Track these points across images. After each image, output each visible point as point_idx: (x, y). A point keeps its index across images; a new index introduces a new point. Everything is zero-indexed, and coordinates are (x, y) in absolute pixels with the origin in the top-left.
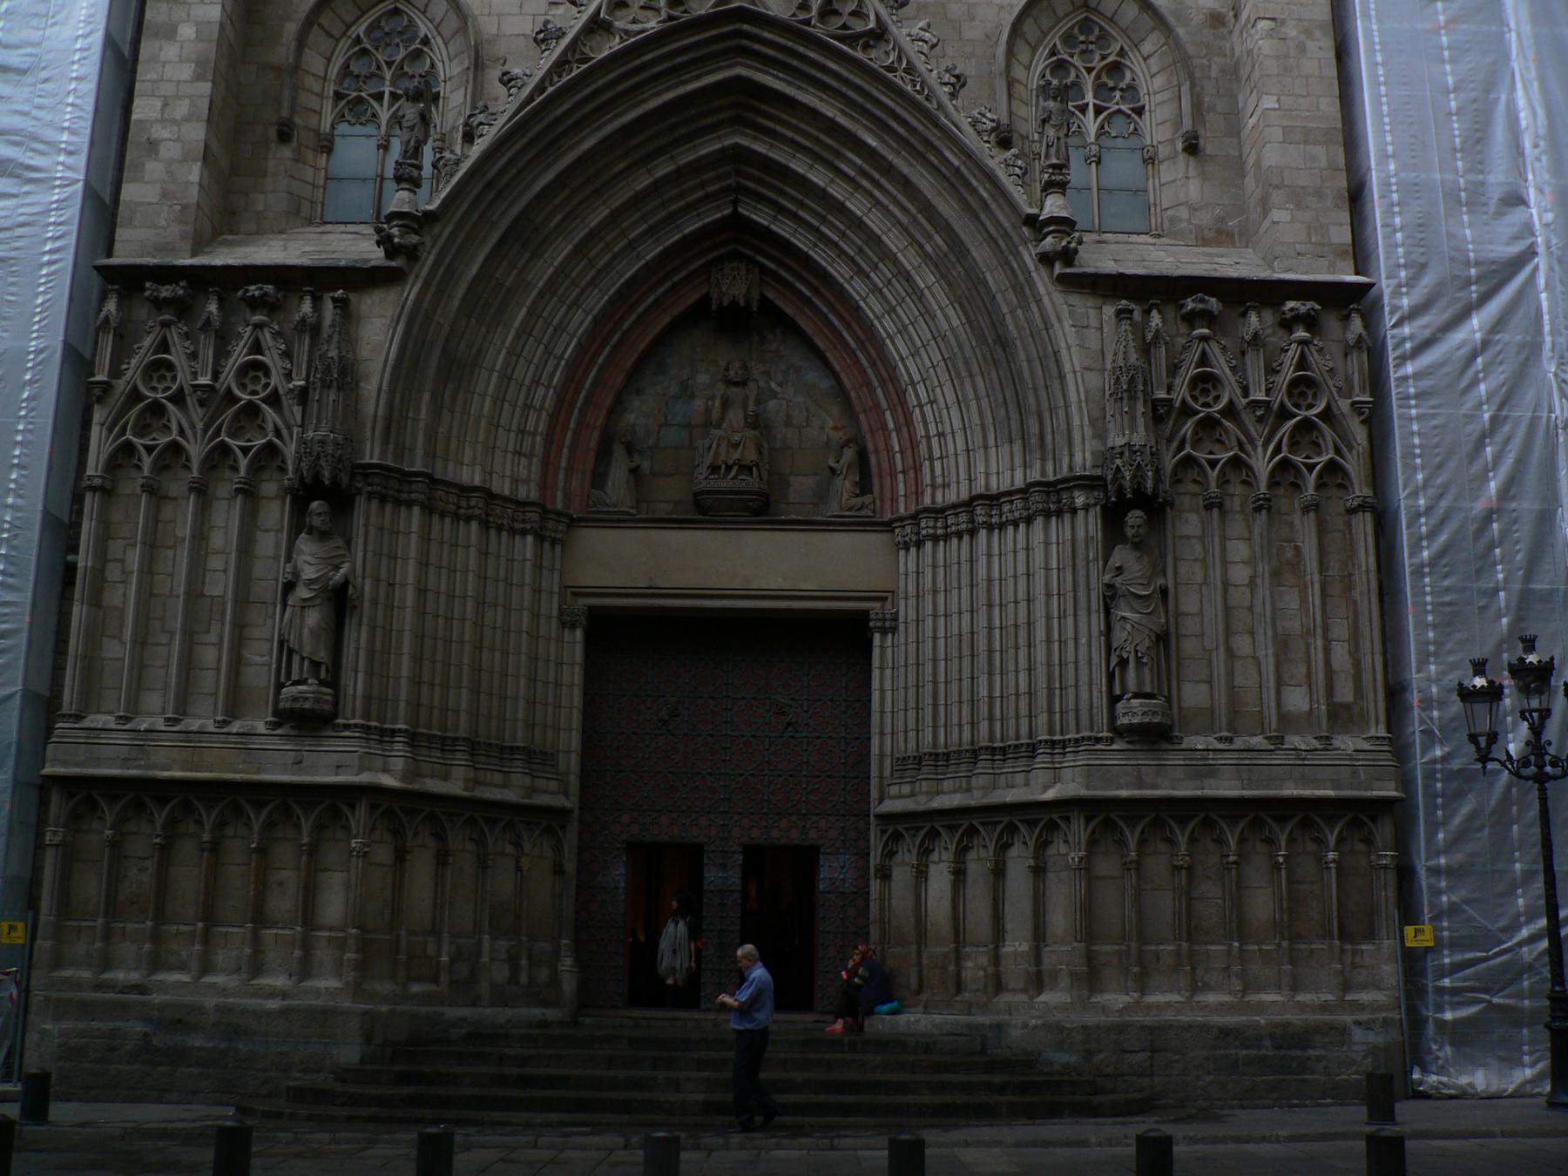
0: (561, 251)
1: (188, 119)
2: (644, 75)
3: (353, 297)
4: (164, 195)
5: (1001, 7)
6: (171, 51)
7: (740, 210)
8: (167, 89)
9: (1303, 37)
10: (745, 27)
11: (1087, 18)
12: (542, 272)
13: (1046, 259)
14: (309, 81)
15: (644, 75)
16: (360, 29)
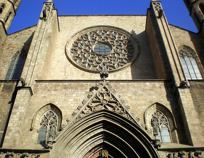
0: (76, 147)
1: (17, 126)
2: (89, 120)
3: (41, 155)
4: (11, 138)
5: (144, 109)
6: (15, 116)
7: (105, 141)
8: (14, 122)
9: (191, 110)
10: (105, 112)
11: (157, 110)
12: (72, 151)
13: (156, 147)
14: (36, 122)
15: (89, 120)
16: (45, 114)
